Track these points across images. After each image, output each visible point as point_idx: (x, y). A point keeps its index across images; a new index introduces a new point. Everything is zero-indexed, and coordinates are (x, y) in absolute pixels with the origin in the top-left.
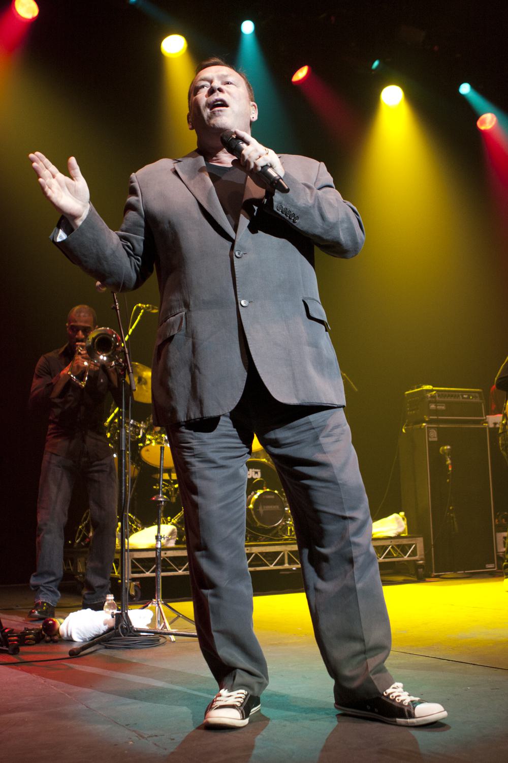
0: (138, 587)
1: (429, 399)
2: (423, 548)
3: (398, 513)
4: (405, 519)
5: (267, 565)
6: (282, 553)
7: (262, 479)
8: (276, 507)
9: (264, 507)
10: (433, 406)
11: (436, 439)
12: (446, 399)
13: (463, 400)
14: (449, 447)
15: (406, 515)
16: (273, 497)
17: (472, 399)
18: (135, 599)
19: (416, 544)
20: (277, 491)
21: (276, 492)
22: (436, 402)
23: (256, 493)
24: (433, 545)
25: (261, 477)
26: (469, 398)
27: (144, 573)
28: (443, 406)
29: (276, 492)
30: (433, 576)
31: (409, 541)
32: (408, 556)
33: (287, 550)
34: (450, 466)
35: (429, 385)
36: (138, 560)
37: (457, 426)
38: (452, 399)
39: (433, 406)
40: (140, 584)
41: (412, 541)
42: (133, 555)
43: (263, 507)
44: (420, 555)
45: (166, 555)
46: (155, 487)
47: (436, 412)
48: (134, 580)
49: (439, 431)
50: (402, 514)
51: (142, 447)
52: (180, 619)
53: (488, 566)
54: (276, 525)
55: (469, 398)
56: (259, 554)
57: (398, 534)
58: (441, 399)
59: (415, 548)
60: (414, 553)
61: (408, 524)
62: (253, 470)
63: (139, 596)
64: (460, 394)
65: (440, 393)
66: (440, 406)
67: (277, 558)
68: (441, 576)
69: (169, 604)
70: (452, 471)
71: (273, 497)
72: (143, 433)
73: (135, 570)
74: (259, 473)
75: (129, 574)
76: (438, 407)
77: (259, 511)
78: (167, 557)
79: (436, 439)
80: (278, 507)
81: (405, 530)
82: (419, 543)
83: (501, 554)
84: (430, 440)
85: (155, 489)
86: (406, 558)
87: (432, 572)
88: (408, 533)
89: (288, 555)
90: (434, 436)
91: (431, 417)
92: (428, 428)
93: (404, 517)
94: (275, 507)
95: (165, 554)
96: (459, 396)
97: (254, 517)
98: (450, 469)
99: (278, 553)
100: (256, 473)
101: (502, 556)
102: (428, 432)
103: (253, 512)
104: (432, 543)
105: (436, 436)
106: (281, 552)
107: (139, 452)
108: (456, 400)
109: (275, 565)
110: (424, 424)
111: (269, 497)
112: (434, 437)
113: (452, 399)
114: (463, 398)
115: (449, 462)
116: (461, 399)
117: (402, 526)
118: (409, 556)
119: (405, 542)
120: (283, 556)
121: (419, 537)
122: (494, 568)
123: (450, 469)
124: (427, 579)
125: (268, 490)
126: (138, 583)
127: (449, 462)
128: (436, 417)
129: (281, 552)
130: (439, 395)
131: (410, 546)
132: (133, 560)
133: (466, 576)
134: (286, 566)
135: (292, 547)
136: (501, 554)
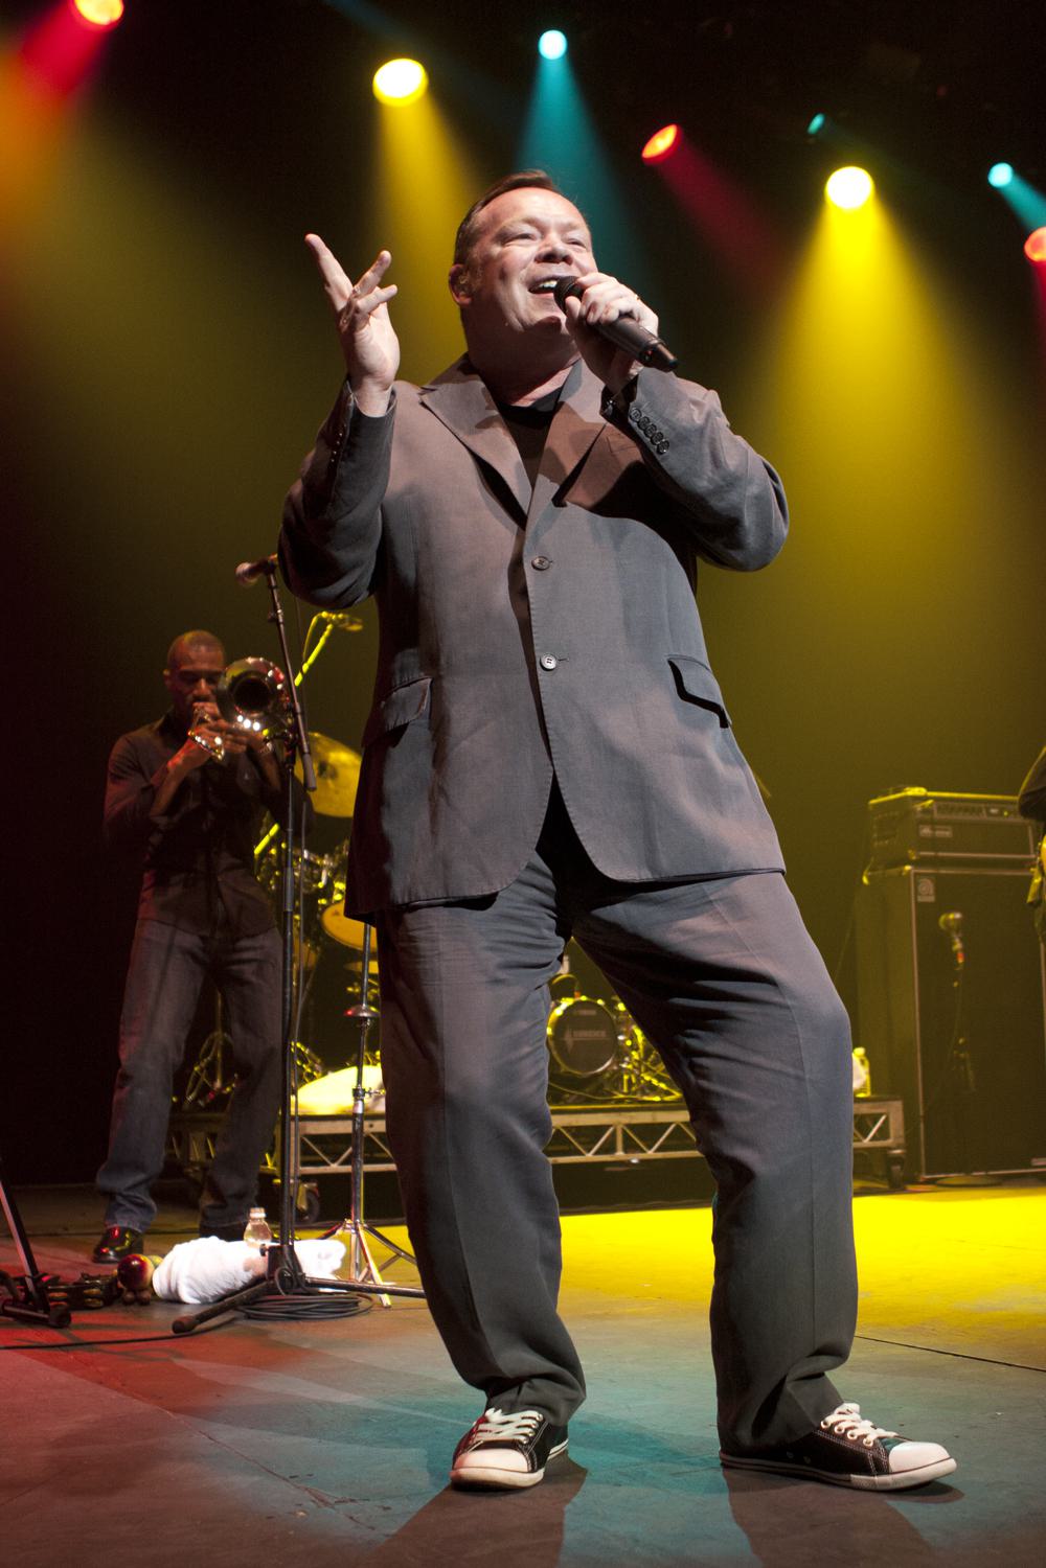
0: (314, 1193)
1: (919, 816)
4: (867, 1063)
5: (580, 1154)
6: (611, 1129)
7: (571, 976)
8: (602, 1034)
9: (575, 1032)
10: (926, 831)
11: (932, 899)
12: (954, 817)
13: (991, 819)
14: (958, 916)
15: (867, 1054)
16: (593, 1013)
17: (1007, 816)
18: (307, 1217)
20: (603, 999)
21: (600, 1002)
22: (933, 823)
23: (558, 1005)
24: (924, 1117)
25: (570, 972)
26: (1000, 814)
27: (324, 1163)
28: (946, 830)
29: (600, 1002)
30: (921, 1180)
32: (872, 1140)
33: (620, 1123)
35: (920, 785)
36: (318, 1139)
38: (968, 817)
39: (926, 831)
40: (318, 1188)
41: (879, 1107)
42: (305, 1128)
44: (896, 1138)
45: (372, 1130)
46: (350, 989)
47: (934, 843)
48: (306, 1178)
49: (940, 883)
51: (325, 907)
52: (401, 1260)
54: (600, 1070)
55: (1000, 814)
56: (564, 1132)
58: (943, 817)
59: (886, 1122)
60: (883, 1133)
63: (317, 1209)
64: (983, 805)
65: (941, 803)
66: (940, 829)
68: (940, 1182)
69: (380, 1230)
70: (965, 963)
71: (593, 1013)
72: (327, 876)
73: (308, 1158)
75: (296, 1168)
77: (564, 1042)
78: (374, 1134)
80: (603, 1034)
81: (864, 1085)
84: (920, 899)
85: (352, 994)
86: (866, 1142)
87: (920, 1172)
88: (873, 1092)
89: (624, 1132)
90: (927, 892)
92: (916, 874)
93: (864, 1058)
94: (596, 1034)
95: (371, 1126)
96: (980, 810)
98: (960, 961)
99: (601, 1129)
102: (917, 884)
104: (921, 1113)
105: (932, 892)
107: (318, 916)
109: (597, 1153)
110: (908, 868)
111: (585, 1012)
112: (928, 895)
114: (989, 814)
115: (958, 946)
116: (984, 817)
118: (873, 1139)
119: (865, 1109)
120: (614, 1134)
121: (896, 1099)
123: (960, 961)
124: (910, 1187)
125: (584, 998)
126: (314, 1185)
127: (958, 946)
128: (932, 854)
129: (608, 1126)
130: (939, 808)
131: (875, 1118)
132: (306, 1140)
133: (989, 1182)
134: (620, 1154)
135: (632, 1117)
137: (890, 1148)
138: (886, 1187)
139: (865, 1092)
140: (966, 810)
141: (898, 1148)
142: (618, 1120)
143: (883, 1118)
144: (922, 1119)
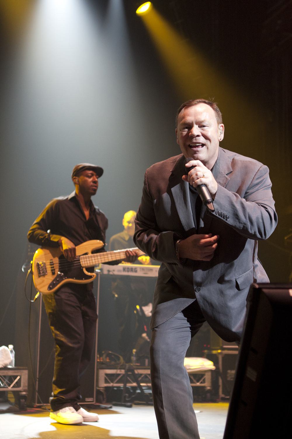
3: (8, 347)
4: (14, 352)
15: (14, 349)
19: (21, 376)
31: (15, 373)
44: (24, 387)
50: (11, 347)
53: (87, 399)
57: (4, 365)
59: (20, 380)
60: (18, 384)
61: (16, 357)
68: (43, 407)
82: (23, 376)
83: (102, 389)
86: (10, 388)
87: (35, 402)
88: (16, 365)
101: (101, 391)
117: (9, 358)
118: (13, 387)
119: (10, 373)
122: (93, 402)
124: (29, 409)
131: (15, 377)
136: (102, 389)
137: (21, 391)
138: (17, 408)
139: (12, 366)
141: (24, 391)
143: (18, 378)
144: (37, 380)
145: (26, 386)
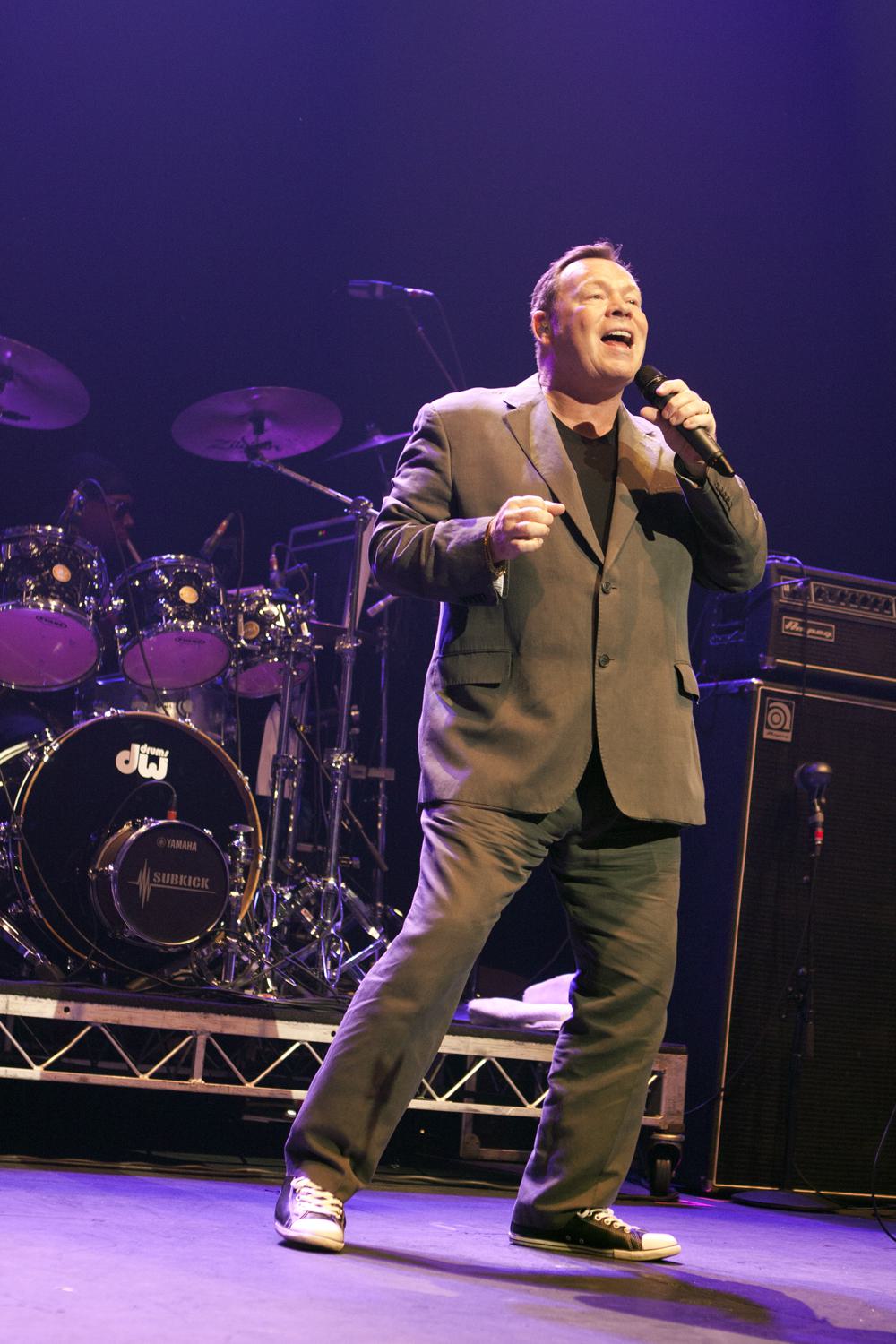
1: (785, 600)
2: (683, 1092)
10: (792, 626)
11: (787, 737)
12: (841, 609)
16: (193, 846)
19: (660, 1075)
21: (207, 831)
22: (804, 615)
28: (828, 629)
29: (207, 831)
34: (820, 830)
37: (865, 703)
38: (864, 613)
39: (792, 626)
43: (152, 877)
44: (669, 1114)
47: (802, 647)
49: (803, 711)
62: (145, 748)
65: (824, 585)
67: (169, 1052)
71: (193, 846)
74: (164, 763)
76: (810, 631)
79: (787, 737)
80: (204, 883)
84: (766, 735)
89: (209, 1045)
91: (778, 661)
94: (193, 881)
97: (117, 904)
100: (153, 759)
103: (114, 890)
105: (787, 727)
106: (190, 1033)
108: (875, 616)
110: (754, 681)
111: (178, 844)
112: (781, 729)
113: (864, 613)
121: (679, 1053)
124: (685, 1200)
127: (820, 817)
130: (819, 594)
134: (197, 1082)
135: (224, 1024)
138: (646, 1193)
140: (865, 601)
142: (201, 1024)
145: (679, 1112)
